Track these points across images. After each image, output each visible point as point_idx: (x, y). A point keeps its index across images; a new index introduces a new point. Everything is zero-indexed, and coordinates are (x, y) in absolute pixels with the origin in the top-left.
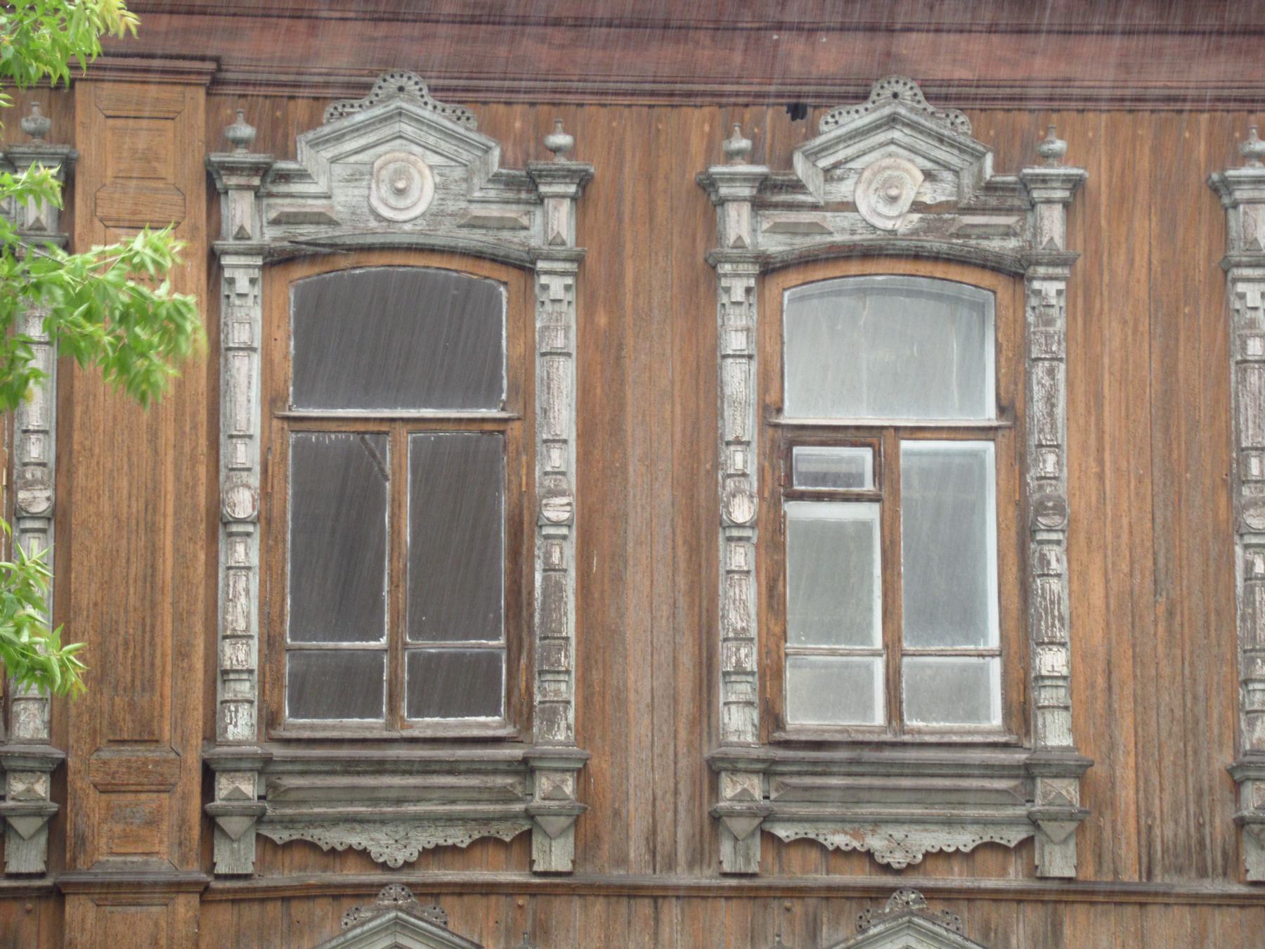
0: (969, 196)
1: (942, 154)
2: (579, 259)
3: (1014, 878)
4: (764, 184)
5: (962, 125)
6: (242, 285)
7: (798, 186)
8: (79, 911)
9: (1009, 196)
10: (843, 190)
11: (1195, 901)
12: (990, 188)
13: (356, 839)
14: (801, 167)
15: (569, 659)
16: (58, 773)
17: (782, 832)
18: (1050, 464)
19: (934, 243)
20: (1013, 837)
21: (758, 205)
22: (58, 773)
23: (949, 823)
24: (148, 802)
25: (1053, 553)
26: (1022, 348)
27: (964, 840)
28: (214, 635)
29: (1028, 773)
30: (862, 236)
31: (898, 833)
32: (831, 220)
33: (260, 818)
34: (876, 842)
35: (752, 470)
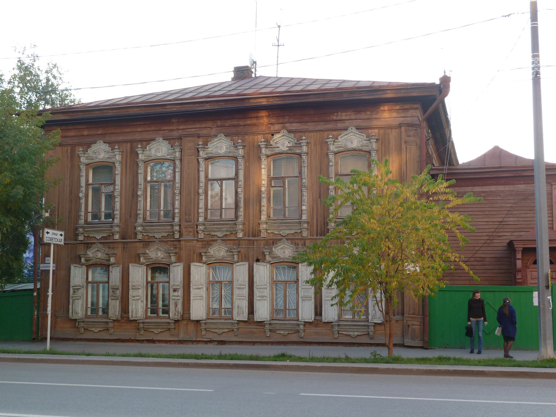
0: (295, 145)
1: (291, 139)
3: (300, 237)
4: (266, 145)
5: (293, 135)
6: (201, 163)
7: (271, 145)
8: (183, 243)
9: (298, 145)
10: (278, 145)
13: (216, 234)
14: (272, 143)
16: (180, 226)
17: (269, 231)
18: (304, 181)
19: (290, 152)
20: (299, 231)
22: (180, 226)
24: (191, 229)
25: (304, 193)
27: (293, 232)
28: (198, 208)
29: (300, 223)
30: (281, 151)
34: (281, 233)
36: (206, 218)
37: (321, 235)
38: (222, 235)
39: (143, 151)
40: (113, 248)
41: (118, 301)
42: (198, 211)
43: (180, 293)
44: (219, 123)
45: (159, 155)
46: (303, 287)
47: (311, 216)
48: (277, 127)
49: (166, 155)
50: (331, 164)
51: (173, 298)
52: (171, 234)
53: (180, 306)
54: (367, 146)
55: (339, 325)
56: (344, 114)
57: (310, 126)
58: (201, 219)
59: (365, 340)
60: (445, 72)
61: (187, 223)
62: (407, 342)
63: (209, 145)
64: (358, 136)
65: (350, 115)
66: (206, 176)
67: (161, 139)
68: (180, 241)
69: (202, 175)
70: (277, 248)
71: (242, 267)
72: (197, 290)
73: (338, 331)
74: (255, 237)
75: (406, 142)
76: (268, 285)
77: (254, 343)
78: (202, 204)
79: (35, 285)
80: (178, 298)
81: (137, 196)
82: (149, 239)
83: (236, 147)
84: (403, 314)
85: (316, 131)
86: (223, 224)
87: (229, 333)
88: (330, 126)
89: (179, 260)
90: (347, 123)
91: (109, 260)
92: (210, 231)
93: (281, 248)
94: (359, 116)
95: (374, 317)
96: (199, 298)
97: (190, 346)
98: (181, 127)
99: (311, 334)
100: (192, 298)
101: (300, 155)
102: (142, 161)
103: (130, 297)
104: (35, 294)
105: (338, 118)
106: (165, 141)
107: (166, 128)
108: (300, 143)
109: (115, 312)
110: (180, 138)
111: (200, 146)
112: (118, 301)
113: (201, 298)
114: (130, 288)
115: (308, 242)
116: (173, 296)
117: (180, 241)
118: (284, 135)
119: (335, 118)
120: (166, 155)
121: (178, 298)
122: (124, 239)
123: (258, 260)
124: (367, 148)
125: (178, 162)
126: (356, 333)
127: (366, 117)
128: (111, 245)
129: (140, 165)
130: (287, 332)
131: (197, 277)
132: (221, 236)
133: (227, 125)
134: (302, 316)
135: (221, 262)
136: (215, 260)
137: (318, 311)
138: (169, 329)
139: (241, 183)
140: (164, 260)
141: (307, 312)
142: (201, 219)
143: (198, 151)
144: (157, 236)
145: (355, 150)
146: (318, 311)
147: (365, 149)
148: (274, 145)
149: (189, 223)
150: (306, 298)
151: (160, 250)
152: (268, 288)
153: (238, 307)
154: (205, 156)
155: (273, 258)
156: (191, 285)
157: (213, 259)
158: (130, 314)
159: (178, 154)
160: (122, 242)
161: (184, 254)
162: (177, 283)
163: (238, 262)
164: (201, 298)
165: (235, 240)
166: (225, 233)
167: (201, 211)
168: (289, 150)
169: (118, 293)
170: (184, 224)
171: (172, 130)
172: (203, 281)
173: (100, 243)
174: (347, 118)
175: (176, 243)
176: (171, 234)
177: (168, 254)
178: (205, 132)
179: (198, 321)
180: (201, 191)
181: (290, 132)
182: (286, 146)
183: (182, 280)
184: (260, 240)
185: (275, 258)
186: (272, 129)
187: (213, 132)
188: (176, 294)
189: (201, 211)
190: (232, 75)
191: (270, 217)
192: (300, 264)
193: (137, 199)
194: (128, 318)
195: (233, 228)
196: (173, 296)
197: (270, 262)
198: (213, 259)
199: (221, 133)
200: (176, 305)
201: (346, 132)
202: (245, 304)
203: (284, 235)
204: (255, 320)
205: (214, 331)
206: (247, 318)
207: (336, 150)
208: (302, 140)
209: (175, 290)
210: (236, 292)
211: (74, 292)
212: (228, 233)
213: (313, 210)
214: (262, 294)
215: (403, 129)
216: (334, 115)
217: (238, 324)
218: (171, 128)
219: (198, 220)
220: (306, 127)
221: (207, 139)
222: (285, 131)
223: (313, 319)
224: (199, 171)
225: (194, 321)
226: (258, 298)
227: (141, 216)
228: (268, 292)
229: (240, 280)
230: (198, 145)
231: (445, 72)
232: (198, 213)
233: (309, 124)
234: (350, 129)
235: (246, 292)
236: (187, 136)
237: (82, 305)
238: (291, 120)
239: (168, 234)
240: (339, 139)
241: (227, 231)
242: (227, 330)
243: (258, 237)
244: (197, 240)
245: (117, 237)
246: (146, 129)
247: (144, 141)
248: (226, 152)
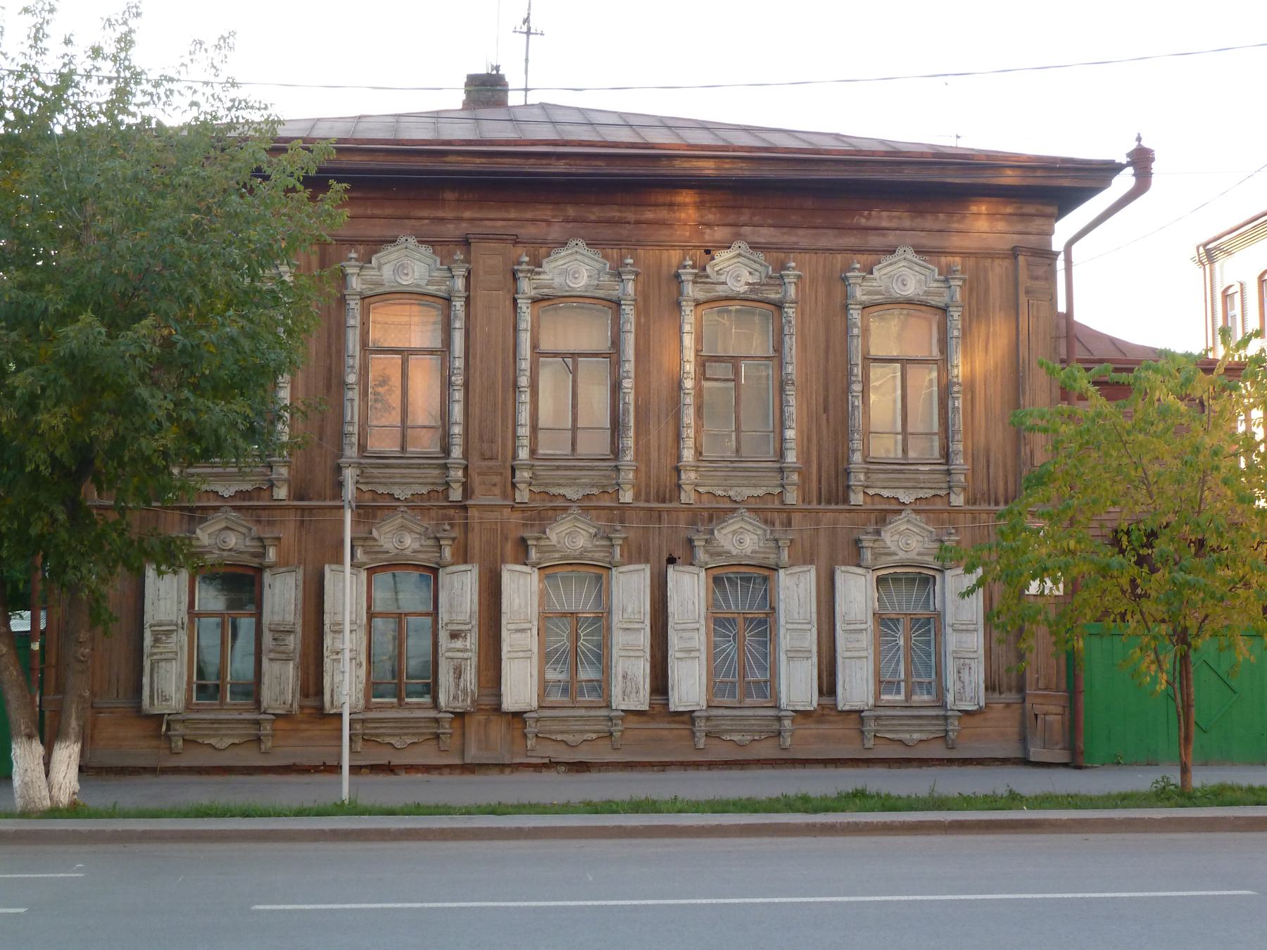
0: (764, 281)
2: (635, 300)
3: (777, 505)
4: (696, 275)
5: (760, 256)
6: (524, 309)
7: (707, 277)
8: (473, 513)
10: (722, 278)
11: (835, 511)
12: (771, 277)
13: (562, 491)
14: (708, 269)
15: (632, 433)
16: (466, 468)
18: (790, 369)
19: (753, 297)
21: (695, 282)
23: (755, 486)
24: (496, 479)
26: (782, 329)
27: (761, 492)
28: (515, 425)
30: (729, 294)
31: (739, 489)
32: (719, 288)
33: (530, 484)
34: (731, 493)
35: (692, 371)
36: (533, 452)
37: (829, 502)
38: (580, 496)
39: (361, 268)
40: (271, 523)
41: (291, 665)
42: (515, 431)
43: (471, 642)
44: (571, 212)
45: (406, 281)
46: (789, 626)
47: (805, 455)
48: (720, 233)
49: (423, 283)
50: (856, 331)
51: (449, 654)
52: (440, 489)
53: (470, 676)
54: (940, 295)
55: (877, 718)
56: (885, 214)
57: (802, 238)
58: (523, 454)
59: (939, 751)
60: (1139, 139)
61: (486, 463)
62: (1036, 753)
63: (544, 264)
64: (917, 268)
65: (900, 218)
66: (534, 346)
67: (412, 241)
68: (465, 508)
69: (525, 339)
70: (724, 531)
71: (635, 577)
72: (518, 635)
73: (877, 731)
74: (664, 501)
75: (1027, 292)
76: (703, 622)
77: (664, 766)
78: (524, 416)
79: (34, 621)
80: (466, 655)
81: (343, 384)
82: (374, 500)
83: (620, 274)
84: (1021, 689)
85: (816, 251)
86: (582, 469)
87: (600, 742)
88: (851, 240)
89: (464, 556)
90: (891, 238)
91: (263, 555)
92: (547, 485)
93: (734, 532)
94: (919, 222)
95: (959, 697)
96: (521, 654)
97: (494, 777)
98: (467, 214)
99: (795, 740)
100: (504, 655)
101: (779, 306)
102: (360, 294)
103: (326, 654)
104: (36, 646)
105: (872, 223)
106: (423, 248)
107: (425, 213)
108: (782, 277)
109: (282, 693)
110: (466, 243)
111: (524, 267)
112: (291, 665)
113: (528, 654)
114: (327, 628)
115: (796, 518)
116: (449, 650)
117: (465, 508)
118: (739, 255)
119: (863, 221)
120: (423, 283)
121: (466, 655)
122: (302, 499)
123: (671, 560)
124: (938, 299)
125: (459, 305)
126: (916, 736)
127: (937, 226)
128: (264, 516)
129: (352, 304)
130: (749, 738)
131: (517, 601)
132: (575, 497)
133: (593, 217)
134: (788, 697)
135: (575, 564)
136: (561, 559)
137: (828, 686)
138: (437, 736)
139: (629, 367)
140: (421, 556)
141: (798, 686)
142: (523, 454)
143: (515, 279)
144: (397, 492)
145: (909, 302)
146: (828, 686)
147: (935, 300)
148: (714, 278)
149: (491, 463)
150: (797, 654)
151: (411, 531)
152: (703, 630)
153: (624, 677)
154: (533, 293)
155: (711, 555)
156: (504, 622)
157: (557, 555)
158: (327, 697)
159: (460, 283)
160: (296, 508)
161: (476, 542)
162: (462, 617)
163: (623, 564)
164: (528, 654)
165: (611, 508)
166: (588, 491)
167: (524, 431)
168: (751, 291)
169: (293, 642)
170: (475, 462)
171: (442, 219)
172: (533, 611)
173: (235, 508)
174: (893, 224)
175: (452, 512)
176: (440, 489)
177: (431, 542)
178: (530, 231)
179: (518, 715)
180: (524, 381)
181: (754, 247)
182: (743, 282)
183: (476, 607)
184: (676, 510)
185: (719, 554)
186: (707, 237)
187: (555, 232)
188: (459, 644)
189: (524, 431)
190: (462, 96)
191: (701, 454)
192: (781, 572)
193: (341, 395)
194: (322, 707)
195: (608, 477)
196: (449, 650)
197: (707, 563)
198: (557, 555)
199: (576, 236)
200: (458, 673)
201: (891, 259)
202: (641, 669)
203: (738, 499)
204: (672, 708)
205: (559, 737)
206: (647, 701)
207: (864, 298)
208: (788, 269)
209: (454, 636)
210: (619, 639)
211: (156, 640)
212: (595, 491)
213: (809, 440)
214: (688, 645)
215: (1021, 259)
216: (862, 216)
217: (622, 719)
218: (440, 214)
219: (515, 457)
220: (794, 239)
221: (540, 251)
222: (744, 245)
223: (815, 704)
224: (516, 329)
225: (507, 713)
226: (678, 655)
227: (355, 439)
228: (703, 638)
229: (630, 610)
230: (520, 263)
231: (1139, 139)
232: (515, 437)
233: (801, 232)
234: (900, 251)
235: (643, 639)
236: (485, 238)
237: (180, 676)
238: (756, 219)
239: (430, 488)
240: (876, 274)
241: (593, 486)
242: (594, 736)
243: (671, 501)
244: (513, 507)
245: (282, 493)
246: (369, 212)
247: (361, 242)
248: (587, 286)
